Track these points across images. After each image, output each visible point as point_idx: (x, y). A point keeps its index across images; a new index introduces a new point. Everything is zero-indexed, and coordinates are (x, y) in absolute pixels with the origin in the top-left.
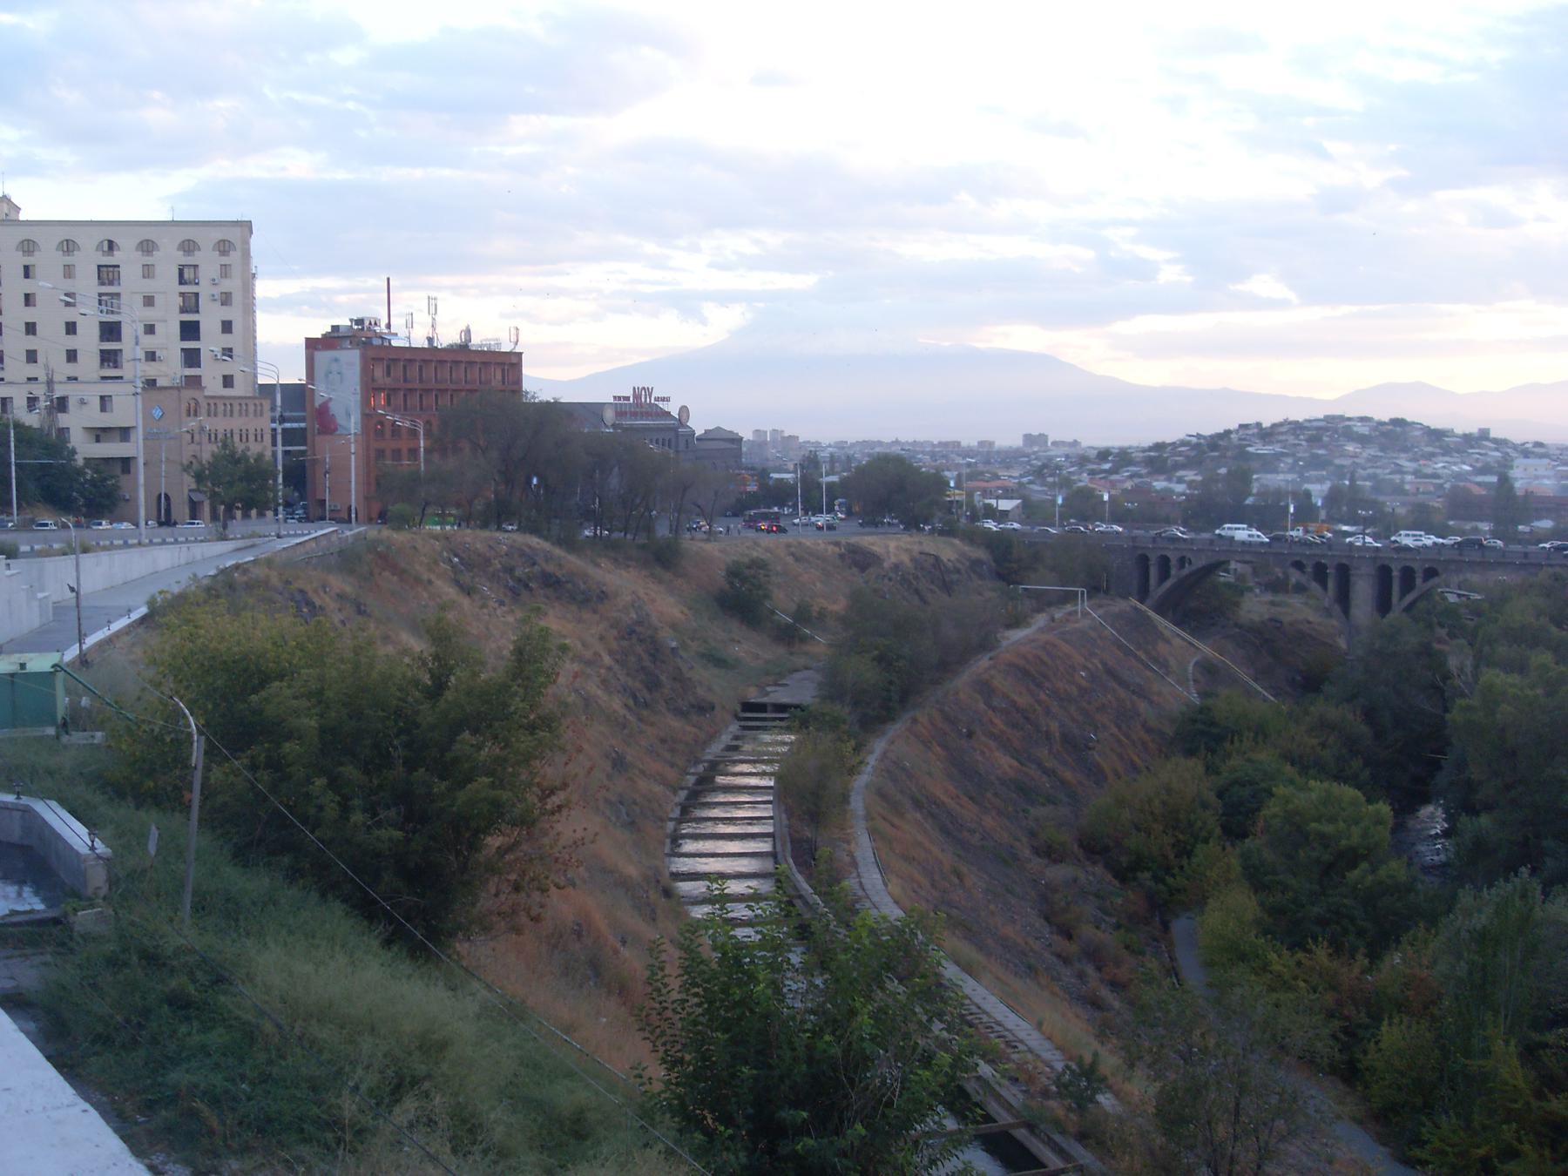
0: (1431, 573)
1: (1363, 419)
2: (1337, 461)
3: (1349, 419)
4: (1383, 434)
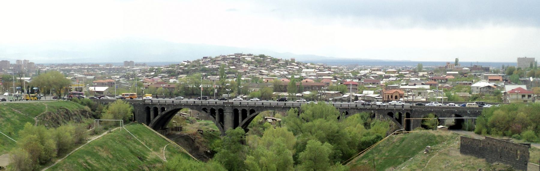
0: (252, 111)
1: (250, 55)
2: (239, 71)
3: (244, 55)
4: (256, 61)
